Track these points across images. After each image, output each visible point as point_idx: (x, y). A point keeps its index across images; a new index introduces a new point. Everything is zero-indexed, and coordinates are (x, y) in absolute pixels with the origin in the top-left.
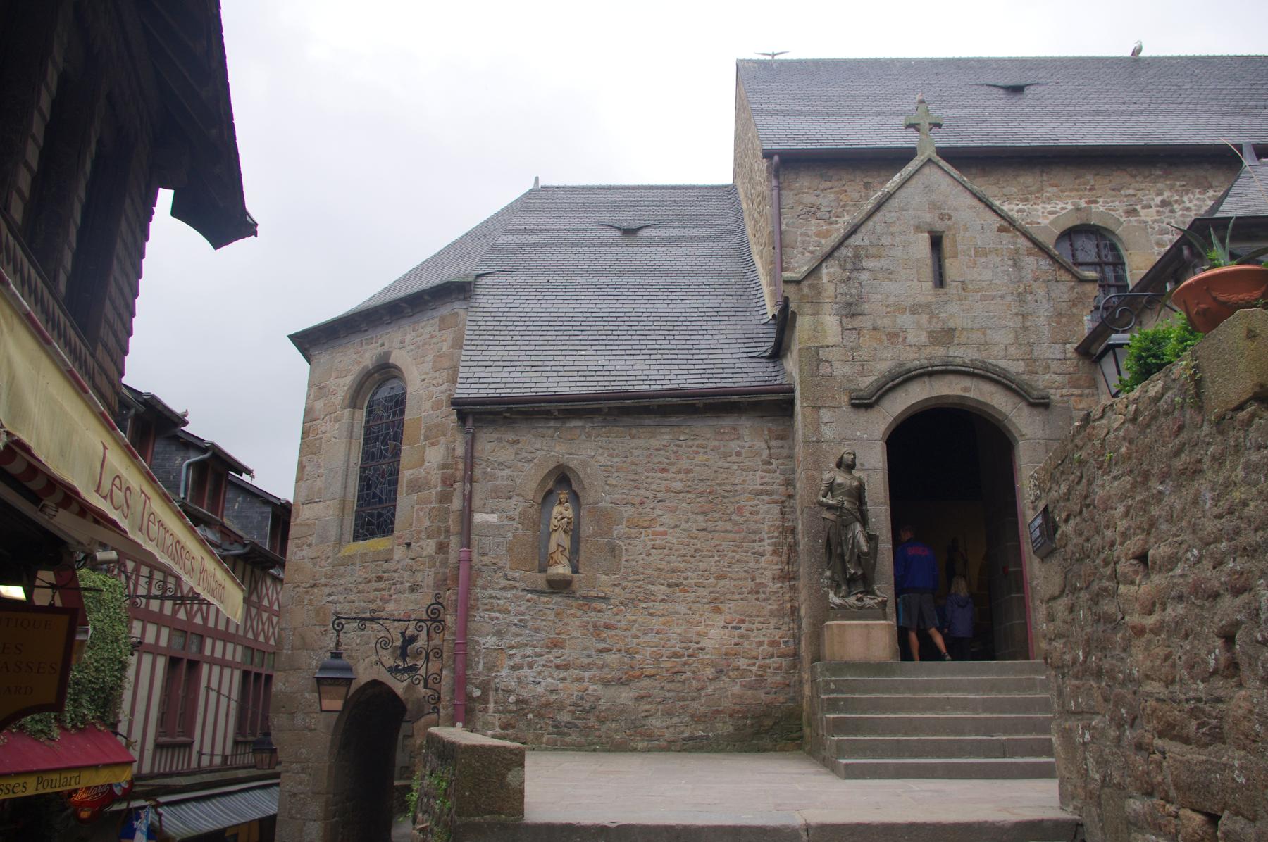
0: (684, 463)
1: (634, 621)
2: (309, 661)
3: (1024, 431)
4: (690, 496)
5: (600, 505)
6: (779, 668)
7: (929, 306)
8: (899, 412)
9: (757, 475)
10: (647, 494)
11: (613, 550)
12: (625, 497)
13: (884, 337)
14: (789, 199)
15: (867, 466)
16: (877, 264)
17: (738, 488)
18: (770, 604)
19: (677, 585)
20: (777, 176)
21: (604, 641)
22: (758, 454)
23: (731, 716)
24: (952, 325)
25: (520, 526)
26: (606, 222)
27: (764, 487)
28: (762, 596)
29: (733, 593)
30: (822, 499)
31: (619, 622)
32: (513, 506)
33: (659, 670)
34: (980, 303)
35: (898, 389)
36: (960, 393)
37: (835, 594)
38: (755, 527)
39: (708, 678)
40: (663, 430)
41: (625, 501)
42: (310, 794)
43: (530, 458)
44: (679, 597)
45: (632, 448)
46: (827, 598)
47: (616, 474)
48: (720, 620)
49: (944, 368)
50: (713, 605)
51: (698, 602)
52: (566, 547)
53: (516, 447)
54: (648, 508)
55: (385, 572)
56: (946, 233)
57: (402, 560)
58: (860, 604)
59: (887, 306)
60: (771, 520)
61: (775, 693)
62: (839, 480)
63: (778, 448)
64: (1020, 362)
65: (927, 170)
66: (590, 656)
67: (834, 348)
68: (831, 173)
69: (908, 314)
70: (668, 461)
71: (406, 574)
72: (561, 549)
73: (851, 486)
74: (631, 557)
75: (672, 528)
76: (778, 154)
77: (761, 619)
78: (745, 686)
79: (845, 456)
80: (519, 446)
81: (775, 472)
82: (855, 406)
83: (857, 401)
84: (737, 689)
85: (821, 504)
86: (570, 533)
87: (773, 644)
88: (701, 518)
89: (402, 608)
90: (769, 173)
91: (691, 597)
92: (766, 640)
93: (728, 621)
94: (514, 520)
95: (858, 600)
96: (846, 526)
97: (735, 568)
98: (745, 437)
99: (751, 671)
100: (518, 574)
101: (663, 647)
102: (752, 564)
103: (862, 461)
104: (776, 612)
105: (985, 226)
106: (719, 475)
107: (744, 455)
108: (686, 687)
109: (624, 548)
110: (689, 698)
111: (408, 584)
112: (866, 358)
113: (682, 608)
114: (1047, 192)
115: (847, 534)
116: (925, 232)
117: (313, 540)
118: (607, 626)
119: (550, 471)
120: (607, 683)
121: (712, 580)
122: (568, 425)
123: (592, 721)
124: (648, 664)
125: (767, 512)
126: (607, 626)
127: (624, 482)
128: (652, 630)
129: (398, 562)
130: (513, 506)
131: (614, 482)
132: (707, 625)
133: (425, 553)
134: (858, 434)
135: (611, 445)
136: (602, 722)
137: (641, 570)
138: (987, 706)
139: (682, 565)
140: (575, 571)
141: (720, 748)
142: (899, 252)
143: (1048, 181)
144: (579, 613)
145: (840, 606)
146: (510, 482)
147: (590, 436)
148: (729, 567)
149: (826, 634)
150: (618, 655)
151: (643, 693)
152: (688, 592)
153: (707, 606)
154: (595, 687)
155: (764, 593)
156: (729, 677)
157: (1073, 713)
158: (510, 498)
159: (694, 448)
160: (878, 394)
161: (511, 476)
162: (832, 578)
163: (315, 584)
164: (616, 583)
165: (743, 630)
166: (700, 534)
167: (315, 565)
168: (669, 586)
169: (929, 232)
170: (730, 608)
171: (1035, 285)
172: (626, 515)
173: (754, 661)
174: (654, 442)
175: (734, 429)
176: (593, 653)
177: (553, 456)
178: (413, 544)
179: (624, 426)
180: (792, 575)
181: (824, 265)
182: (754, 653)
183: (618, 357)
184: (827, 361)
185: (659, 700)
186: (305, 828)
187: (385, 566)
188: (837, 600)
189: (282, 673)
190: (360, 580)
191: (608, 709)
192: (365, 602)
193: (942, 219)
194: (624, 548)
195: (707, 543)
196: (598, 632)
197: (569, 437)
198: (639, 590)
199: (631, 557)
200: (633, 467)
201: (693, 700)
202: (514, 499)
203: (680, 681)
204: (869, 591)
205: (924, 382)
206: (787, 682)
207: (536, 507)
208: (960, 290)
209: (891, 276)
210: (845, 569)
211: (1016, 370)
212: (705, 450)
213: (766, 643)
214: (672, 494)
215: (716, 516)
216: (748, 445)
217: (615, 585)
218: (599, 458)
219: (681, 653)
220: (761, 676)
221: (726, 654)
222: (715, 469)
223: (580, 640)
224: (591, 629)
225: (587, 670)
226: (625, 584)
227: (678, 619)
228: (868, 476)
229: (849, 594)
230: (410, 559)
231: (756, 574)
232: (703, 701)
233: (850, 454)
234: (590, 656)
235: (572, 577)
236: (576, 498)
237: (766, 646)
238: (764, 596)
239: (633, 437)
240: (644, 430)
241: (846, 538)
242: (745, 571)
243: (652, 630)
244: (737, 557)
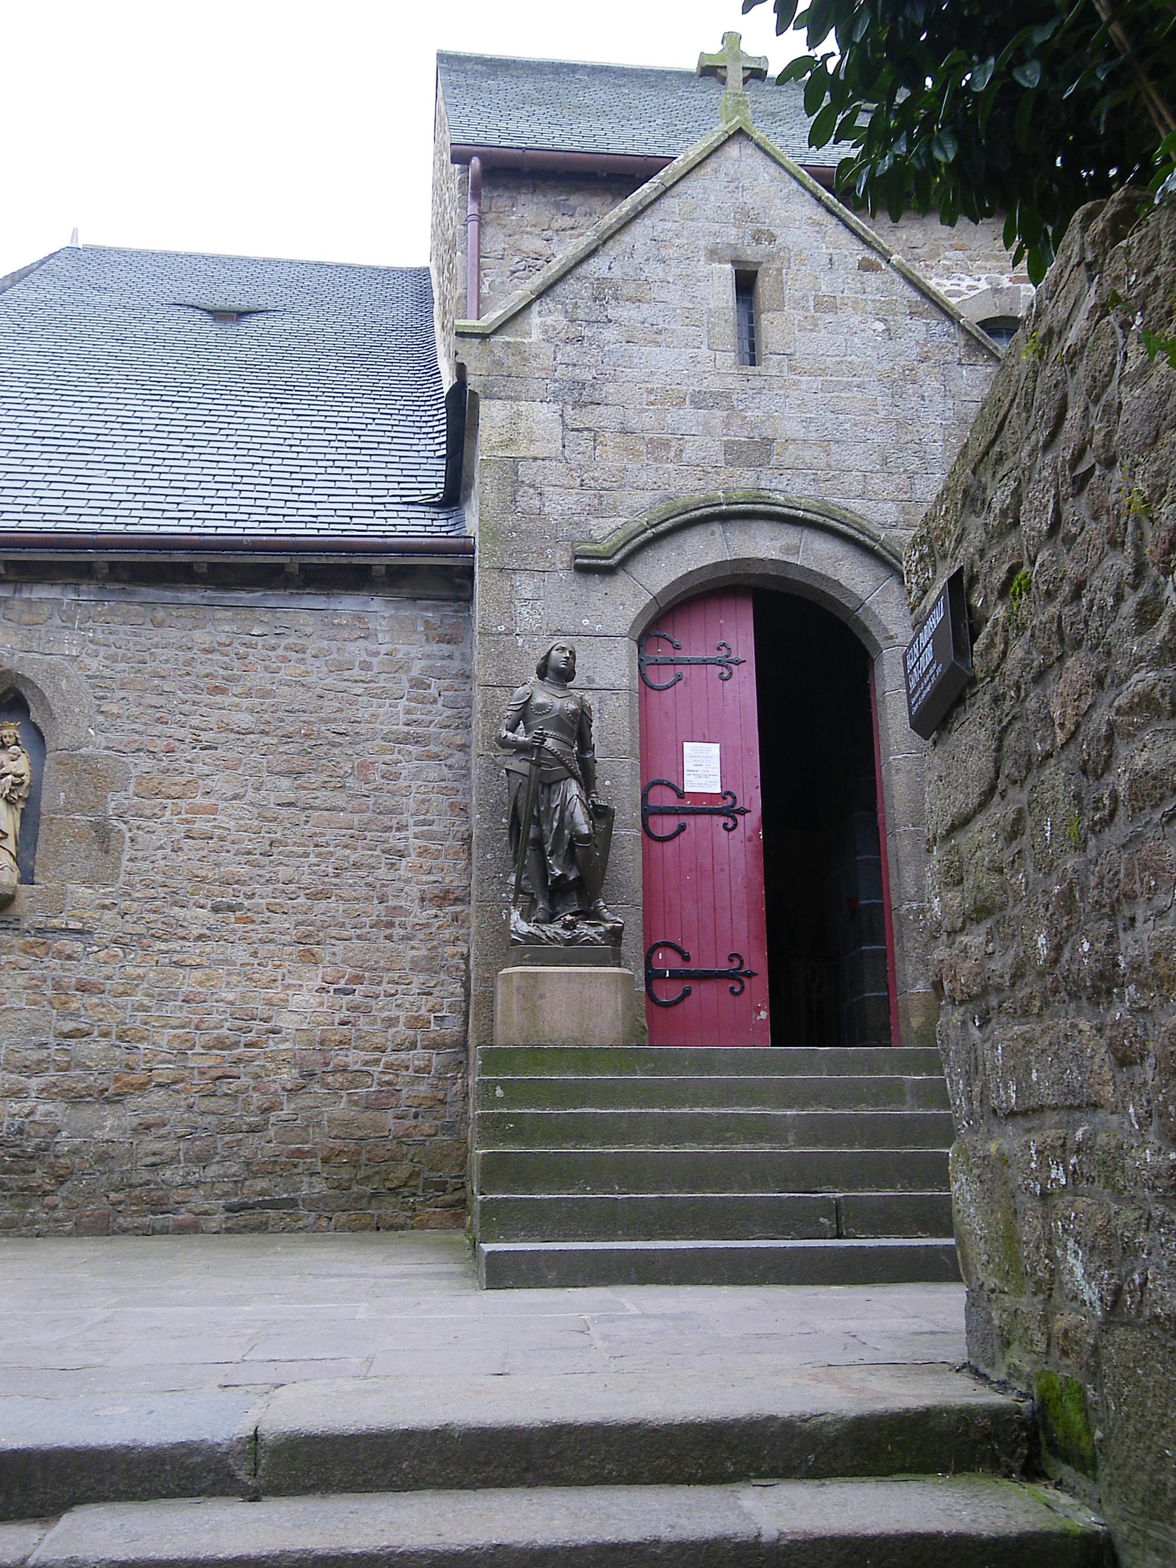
0: (258, 678)
1: (141, 977)
3: (894, 630)
4: (267, 740)
6: (426, 1069)
7: (726, 395)
8: (664, 585)
9: (400, 708)
10: (181, 733)
11: (103, 835)
12: (136, 737)
13: (643, 448)
14: (496, 242)
15: (600, 682)
16: (634, 313)
17: (362, 728)
18: (413, 948)
19: (231, 908)
20: (476, 196)
21: (74, 1015)
22: (403, 667)
23: (325, 1161)
24: (769, 433)
26: (189, 301)
27: (412, 729)
28: (398, 932)
29: (343, 925)
30: (505, 733)
31: (109, 978)
33: (186, 1073)
34: (820, 395)
35: (664, 543)
36: (775, 555)
37: (525, 916)
38: (390, 803)
39: (284, 1089)
40: (220, 614)
41: (136, 746)
44: (233, 931)
45: (156, 647)
46: (507, 923)
47: (122, 694)
48: (314, 978)
49: (750, 507)
50: (301, 947)
51: (271, 941)
54: (182, 762)
56: (764, 265)
58: (567, 934)
59: (650, 391)
60: (422, 789)
61: (416, 1116)
62: (540, 698)
63: (443, 658)
64: (890, 504)
65: (733, 150)
66: (43, 1046)
67: (547, 463)
68: (574, 200)
69: (688, 409)
70: (224, 673)
73: (561, 710)
74: (140, 854)
75: (226, 800)
76: (481, 156)
77: (395, 975)
78: (356, 1103)
79: (554, 653)
81: (435, 701)
82: (584, 570)
83: (586, 561)
84: (341, 1108)
85: (504, 743)
86: (21, 805)
87: (415, 1022)
88: (285, 783)
90: (464, 194)
91: (261, 931)
92: (402, 1015)
93: (329, 979)
95: (566, 927)
96: (549, 784)
97: (348, 878)
98: (380, 636)
99: (369, 1074)
101: (197, 1028)
102: (382, 872)
103: (590, 673)
104: (424, 963)
105: (835, 258)
106: (327, 703)
107: (375, 670)
108: (240, 1104)
109: (128, 835)
110: (245, 1127)
112: (606, 485)
113: (240, 953)
114: (945, 258)
115: (549, 801)
116: (726, 262)
118: (83, 988)
120: (76, 1099)
121: (302, 900)
122: (26, 595)
123: (39, 1177)
124: (161, 1063)
125: (415, 776)
126: (83, 988)
127: (136, 711)
128: (175, 994)
132: (288, 986)
134: (586, 622)
135: (112, 638)
136: (61, 1180)
137: (159, 878)
138: (812, 1131)
139: (244, 871)
140: (27, 877)
141: (301, 1224)
142: (673, 295)
143: (948, 239)
144: (26, 961)
145: (530, 938)
147: (71, 619)
148: (337, 876)
149: (500, 989)
150: (104, 1043)
151: (151, 1118)
152: (253, 922)
153: (289, 949)
154: (50, 1107)
155: (403, 926)
156: (326, 1085)
157: (1012, 1114)
159: (280, 652)
160: (625, 551)
162: (519, 889)
164: (107, 902)
165: (357, 997)
166: (285, 812)
168: (216, 909)
169: (733, 262)
170: (334, 954)
171: (923, 366)
172: (135, 772)
173: (377, 1055)
174: (201, 637)
175: (360, 619)
176: (51, 1039)
179: (141, 604)
180: (458, 893)
181: (536, 308)
182: (378, 1040)
183: (153, 491)
184: (532, 486)
185: (181, 1131)
188: (524, 927)
191: (75, 1152)
193: (758, 241)
194: (128, 835)
195: (297, 829)
196: (63, 997)
197: (26, 618)
198: (153, 917)
199: (140, 854)
200: (156, 682)
201: (253, 1130)
203: (226, 1095)
204: (590, 914)
205: (713, 534)
206: (440, 1096)
208: (785, 369)
209: (660, 338)
210: (544, 868)
211: (879, 518)
212: (300, 656)
213: (402, 1019)
214: (232, 736)
215: (317, 779)
216: (384, 649)
217: (104, 907)
218: (88, 661)
219: (232, 1039)
220: (389, 1083)
221: (322, 1043)
222: (319, 691)
223: (24, 1014)
224: (49, 993)
225: (36, 1074)
226: (124, 905)
227: (229, 974)
228: (601, 701)
229: (551, 919)
231: (389, 891)
232: (272, 1133)
233: (563, 649)
234: (43, 1046)
236: (37, 740)
237: (401, 1027)
238: (402, 932)
239: (159, 625)
240: (182, 612)
241: (548, 808)
242: (368, 885)
243: (175, 994)
244: (353, 857)
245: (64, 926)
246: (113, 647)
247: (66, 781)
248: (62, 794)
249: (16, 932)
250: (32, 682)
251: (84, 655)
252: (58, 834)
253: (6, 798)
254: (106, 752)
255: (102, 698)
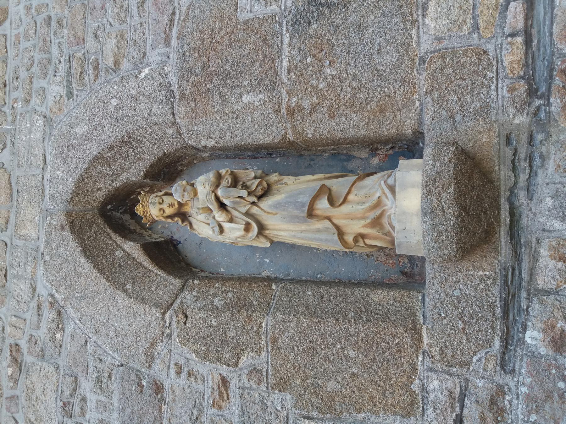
5: (173, 79)
25: (246, 360)
32: (183, 381)
43: (53, 314)
52: (317, 185)
53: (28, 359)
72: (323, 204)
80: (23, 344)
94: (225, 382)
100: (434, 384)
119: (86, 251)
130: (183, 381)
131: (111, 43)
135: (23, 74)
146: (114, 386)
158: (159, 388)
161: (99, 380)
177: (48, 243)
202: (162, 377)
207: (188, 297)
218: (50, 101)
235: (440, 146)
245: (519, 40)
246: (33, 69)
247: (222, 96)
248: (246, 99)
249: (540, 137)
250: (81, 179)
251: (43, 109)
252: (317, 91)
253: (260, 198)
254: (174, 42)
255: (96, 68)
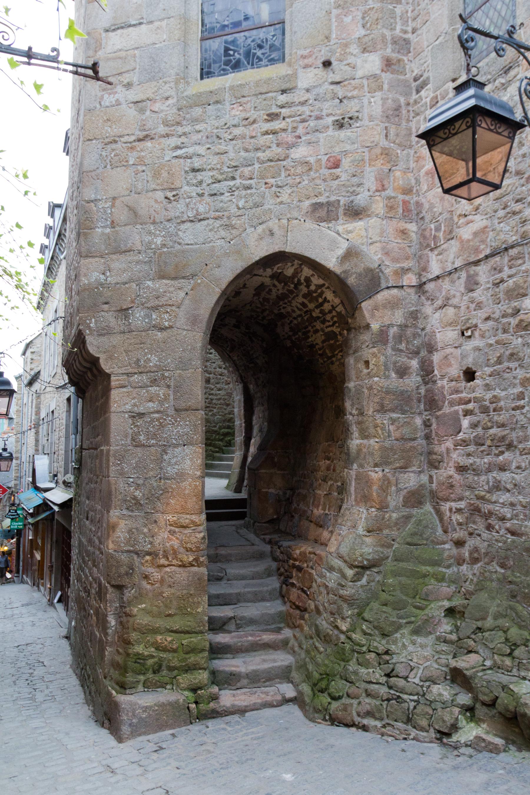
2: (148, 238)
42: (171, 412)
55: (282, 107)
57: (315, 87)
71: (327, 107)
89: (323, 151)
111: (331, 119)
117: (134, 77)
129: (308, 90)
133: (360, 73)
163: (147, 136)
167: (142, 111)
178: (334, 63)
186: (165, 457)
187: (283, 99)
189: (97, 259)
190: (235, 122)
192: (247, 150)
230: (333, 83)
